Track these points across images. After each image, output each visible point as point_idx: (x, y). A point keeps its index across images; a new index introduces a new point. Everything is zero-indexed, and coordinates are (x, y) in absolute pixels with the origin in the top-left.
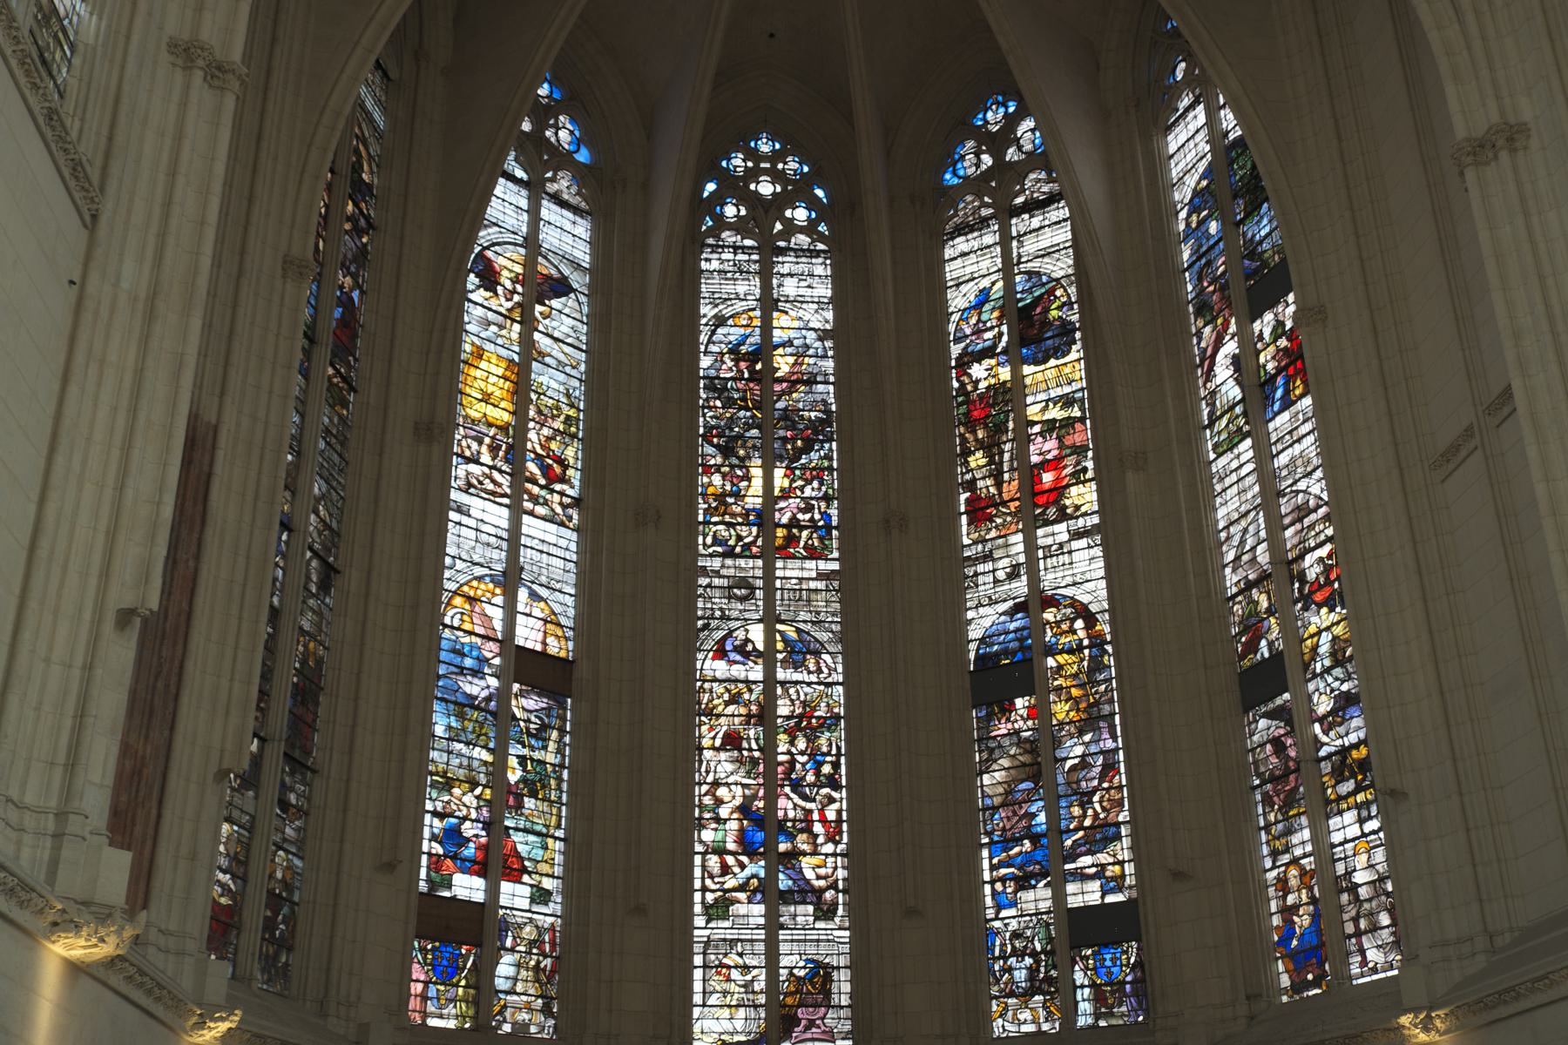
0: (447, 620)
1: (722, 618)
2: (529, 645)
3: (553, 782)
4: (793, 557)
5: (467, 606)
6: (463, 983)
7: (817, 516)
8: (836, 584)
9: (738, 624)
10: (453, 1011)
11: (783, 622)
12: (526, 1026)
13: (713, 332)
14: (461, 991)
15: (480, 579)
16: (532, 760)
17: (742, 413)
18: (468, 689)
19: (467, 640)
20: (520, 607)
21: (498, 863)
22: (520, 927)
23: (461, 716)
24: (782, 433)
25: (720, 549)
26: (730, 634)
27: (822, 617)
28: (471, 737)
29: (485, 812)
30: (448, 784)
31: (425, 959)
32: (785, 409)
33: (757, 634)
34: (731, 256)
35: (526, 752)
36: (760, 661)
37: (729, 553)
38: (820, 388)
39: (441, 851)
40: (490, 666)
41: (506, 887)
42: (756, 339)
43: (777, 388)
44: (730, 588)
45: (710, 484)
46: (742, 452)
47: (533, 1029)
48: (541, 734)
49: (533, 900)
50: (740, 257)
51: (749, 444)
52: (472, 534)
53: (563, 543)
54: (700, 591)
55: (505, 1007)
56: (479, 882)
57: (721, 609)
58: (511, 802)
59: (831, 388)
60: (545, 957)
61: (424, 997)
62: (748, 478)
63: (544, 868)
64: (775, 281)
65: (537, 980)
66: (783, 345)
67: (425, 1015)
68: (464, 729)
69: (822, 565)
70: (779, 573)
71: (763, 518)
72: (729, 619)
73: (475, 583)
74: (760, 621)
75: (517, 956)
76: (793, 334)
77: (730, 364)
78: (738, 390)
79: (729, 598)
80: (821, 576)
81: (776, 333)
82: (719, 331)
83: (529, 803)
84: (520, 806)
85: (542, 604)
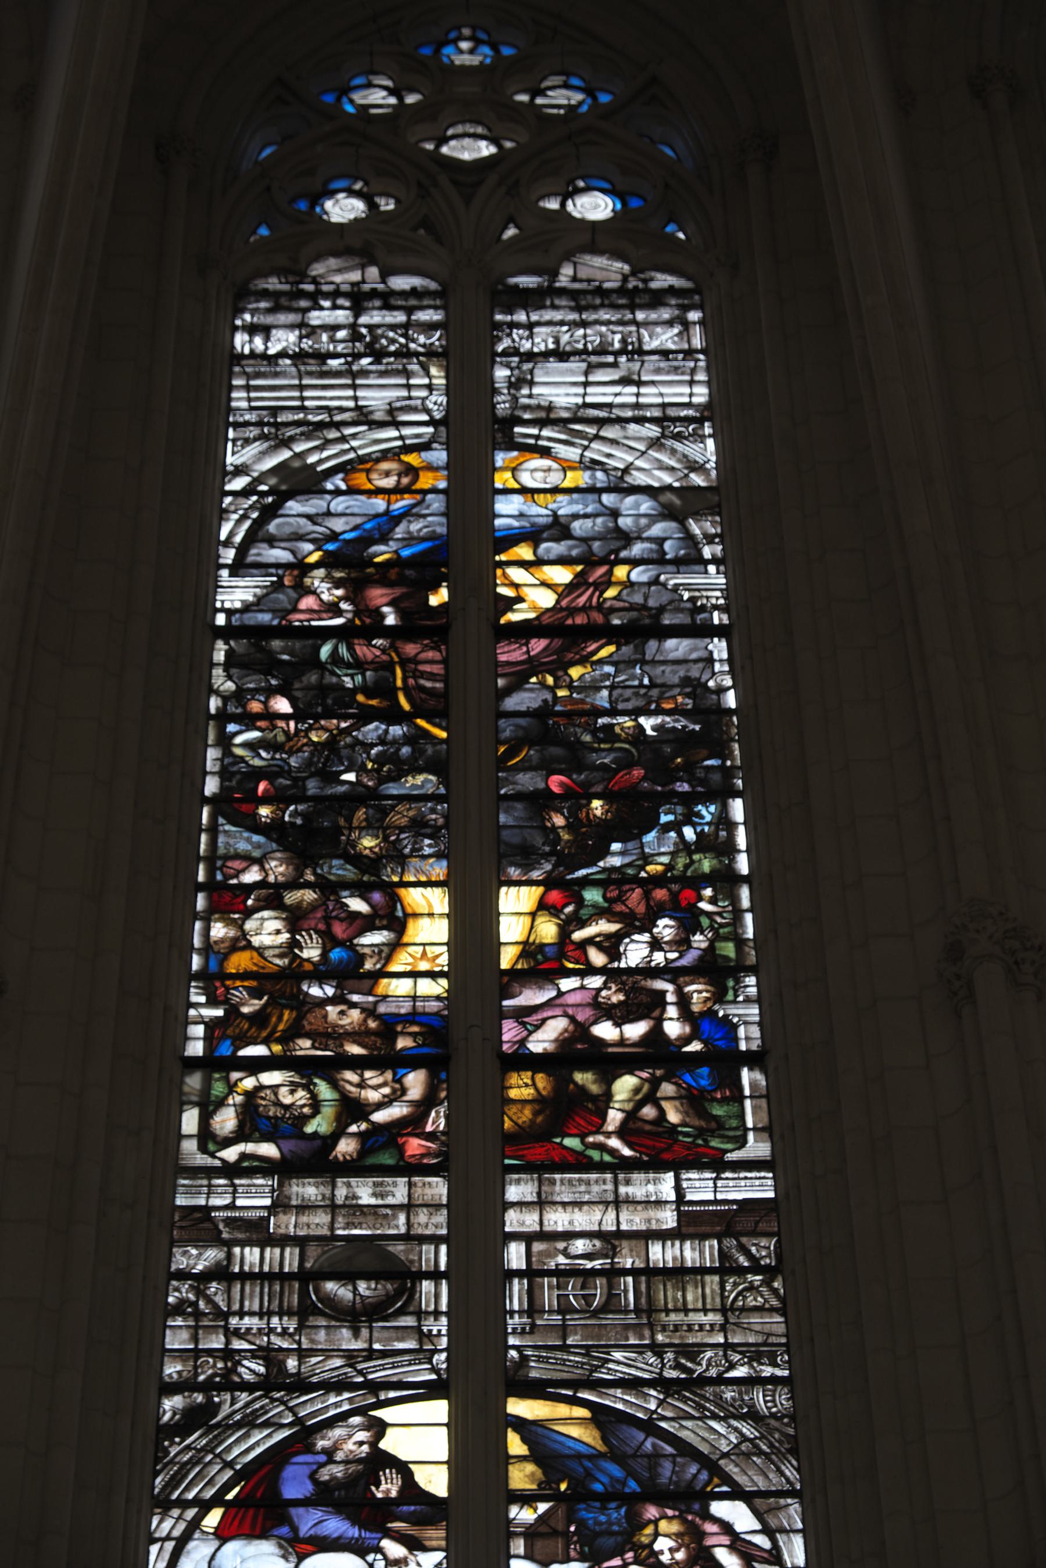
1: (265, 1385)
4: (580, 1163)
7: (673, 1029)
8: (764, 1248)
9: (338, 1402)
11: (536, 1390)
13: (269, 512)
17: (372, 730)
24: (528, 781)
25: (269, 1150)
26: (304, 1435)
27: (707, 1364)
32: (543, 713)
33: (421, 1438)
34: (342, 316)
36: (436, 1535)
37: (314, 1160)
38: (676, 647)
42: (431, 520)
43: (510, 653)
44: (305, 1277)
45: (241, 943)
46: (368, 842)
50: (374, 317)
51: (401, 816)
54: (179, 1293)
57: (268, 1355)
59: (719, 648)
62: (395, 920)
64: (501, 373)
66: (533, 535)
69: (701, 1188)
70: (514, 1221)
71: (455, 1042)
72: (301, 1385)
74: (430, 1391)
76: (565, 506)
77: (328, 593)
78: (359, 665)
79: (305, 1312)
80: (693, 1223)
81: (507, 507)
82: (293, 506)
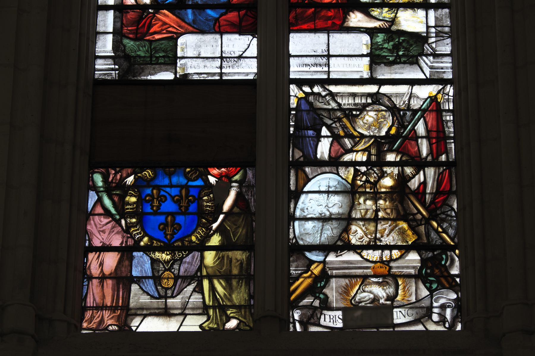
6: (215, 240)
14: (210, 257)
22: (351, 115)
41: (300, 43)
49: (376, 58)
55: (325, 276)
60: (420, 165)
61: (123, 279)
65: (402, 214)
67: (126, 312)
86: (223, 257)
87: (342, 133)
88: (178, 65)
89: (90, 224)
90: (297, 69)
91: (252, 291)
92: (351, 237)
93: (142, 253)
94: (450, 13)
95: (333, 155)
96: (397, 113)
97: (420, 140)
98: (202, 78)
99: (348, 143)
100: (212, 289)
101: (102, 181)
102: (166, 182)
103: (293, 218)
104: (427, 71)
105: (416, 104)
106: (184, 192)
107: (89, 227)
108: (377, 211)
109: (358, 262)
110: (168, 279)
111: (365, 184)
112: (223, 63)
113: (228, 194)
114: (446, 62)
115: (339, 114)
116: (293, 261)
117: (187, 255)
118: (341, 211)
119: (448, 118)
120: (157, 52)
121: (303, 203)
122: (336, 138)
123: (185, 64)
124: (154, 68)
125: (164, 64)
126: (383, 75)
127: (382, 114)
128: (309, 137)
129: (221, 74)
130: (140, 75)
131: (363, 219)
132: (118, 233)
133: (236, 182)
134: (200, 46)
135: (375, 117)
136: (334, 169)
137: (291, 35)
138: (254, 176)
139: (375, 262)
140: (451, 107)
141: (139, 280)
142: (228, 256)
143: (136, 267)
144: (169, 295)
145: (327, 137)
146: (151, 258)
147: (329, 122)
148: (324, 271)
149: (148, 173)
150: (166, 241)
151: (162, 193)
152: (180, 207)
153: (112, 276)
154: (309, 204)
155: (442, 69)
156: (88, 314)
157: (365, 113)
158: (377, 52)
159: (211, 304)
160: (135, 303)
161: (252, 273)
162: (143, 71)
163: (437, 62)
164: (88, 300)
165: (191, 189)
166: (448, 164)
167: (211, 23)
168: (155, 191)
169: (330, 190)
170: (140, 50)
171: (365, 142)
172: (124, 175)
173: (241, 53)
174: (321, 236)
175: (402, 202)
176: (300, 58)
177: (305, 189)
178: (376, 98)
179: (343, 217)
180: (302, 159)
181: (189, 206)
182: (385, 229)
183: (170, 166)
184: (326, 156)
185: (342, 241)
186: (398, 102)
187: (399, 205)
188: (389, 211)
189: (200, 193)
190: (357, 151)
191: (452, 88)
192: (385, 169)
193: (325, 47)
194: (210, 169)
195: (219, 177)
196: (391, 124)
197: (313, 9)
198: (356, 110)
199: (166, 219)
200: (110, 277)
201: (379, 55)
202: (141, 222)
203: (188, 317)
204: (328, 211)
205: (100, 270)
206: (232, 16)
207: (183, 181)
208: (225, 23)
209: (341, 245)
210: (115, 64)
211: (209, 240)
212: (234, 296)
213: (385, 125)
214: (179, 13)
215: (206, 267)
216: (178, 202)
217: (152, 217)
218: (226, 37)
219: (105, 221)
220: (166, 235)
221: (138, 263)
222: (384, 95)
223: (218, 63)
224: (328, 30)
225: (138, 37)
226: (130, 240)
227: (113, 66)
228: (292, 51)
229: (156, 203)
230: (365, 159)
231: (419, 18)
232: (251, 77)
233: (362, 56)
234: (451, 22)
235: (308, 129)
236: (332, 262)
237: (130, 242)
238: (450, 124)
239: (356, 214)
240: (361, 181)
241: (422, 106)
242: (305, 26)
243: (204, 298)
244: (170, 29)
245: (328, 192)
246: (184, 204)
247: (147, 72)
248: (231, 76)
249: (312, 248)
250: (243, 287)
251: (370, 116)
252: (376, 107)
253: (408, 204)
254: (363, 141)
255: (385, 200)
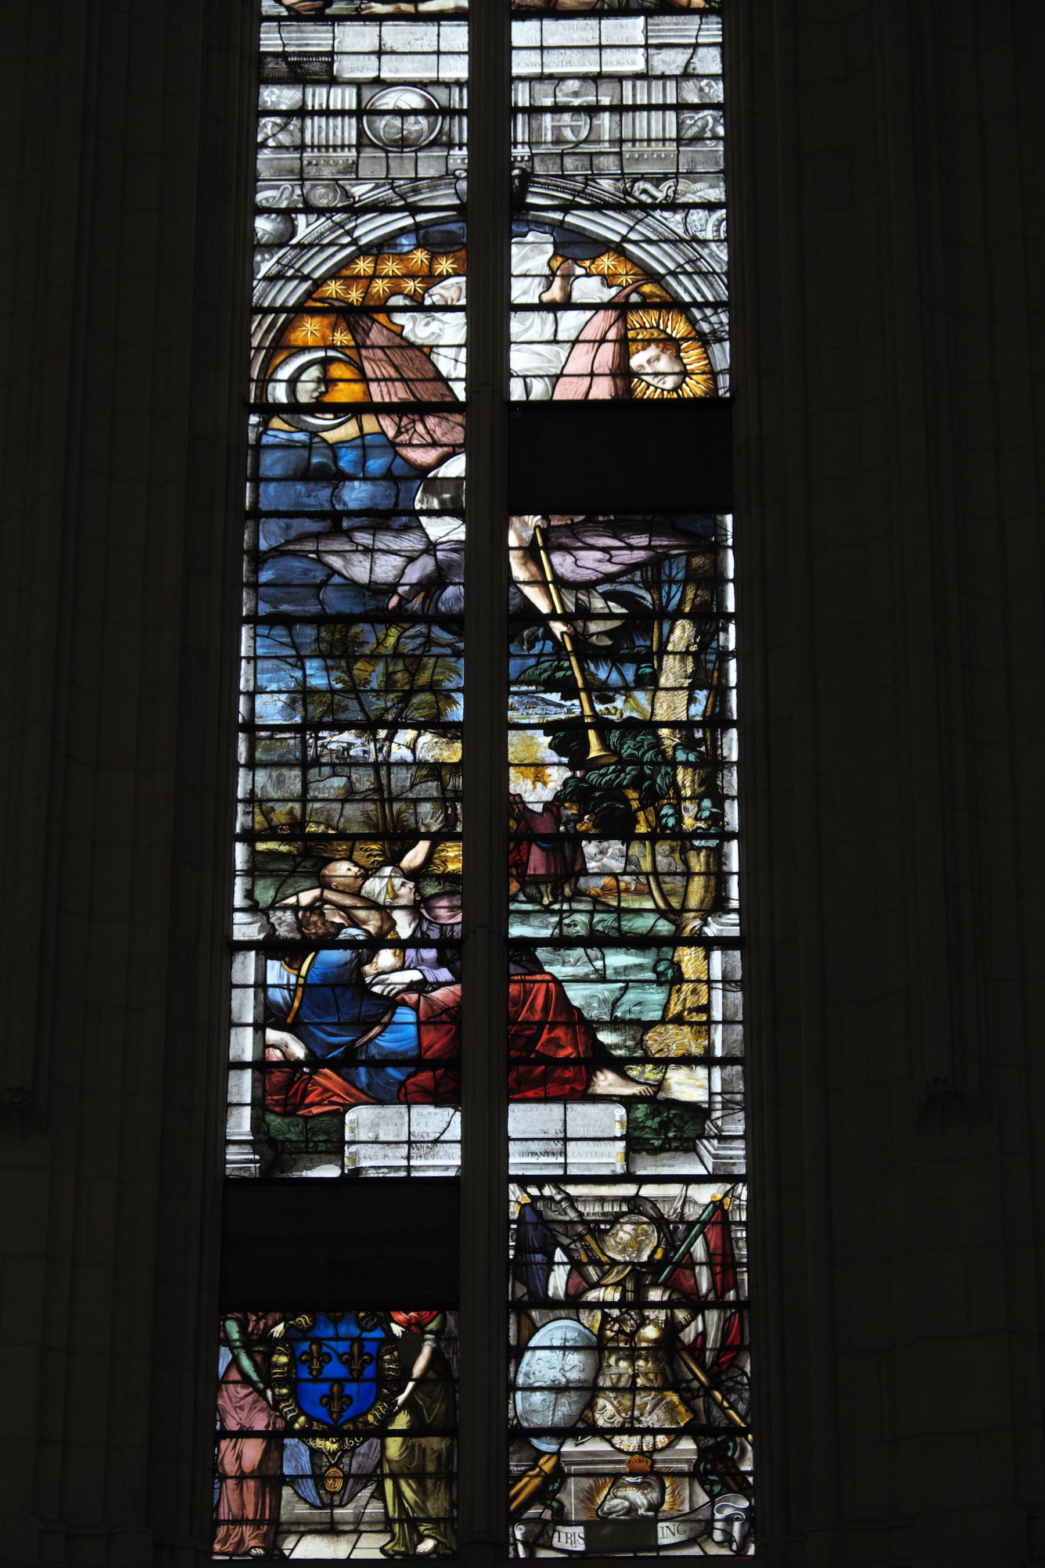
0: (279, 393)
2: (569, 391)
3: (684, 777)
5: (342, 338)
6: (402, 1421)
10: (375, 1509)
12: (640, 1526)
14: (394, 1447)
15: (380, 248)
16: (603, 726)
18: (360, 570)
19: (349, 430)
20: (522, 291)
21: (504, 1046)
22: (599, 1229)
23: (340, 653)
28: (376, 704)
29: (447, 914)
30: (307, 853)
31: (264, 1368)
35: (578, 707)
39: (298, 1050)
40: (433, 486)
41: (525, 1119)
47: (667, 1534)
48: (634, 644)
49: (635, 1143)
52: (347, 130)
53: (671, 62)
55: (559, 1475)
56: (439, 1121)
58: (537, 862)
60: (697, 1306)
63: (679, 1040)
65: (670, 1380)
68: (354, 689)
73: (364, 266)
75: (593, 1319)
83: (602, 856)
84: (568, 870)
85: (606, 263)
86: (413, 1446)
87: (584, 1259)
88: (347, 1154)
89: (223, 1397)
90: (519, 1160)
91: (455, 1497)
92: (597, 1416)
93: (296, 1440)
94: (743, 1072)
95: (572, 1291)
96: (664, 1227)
97: (697, 1268)
98: (381, 1175)
99: (592, 1272)
100: (398, 1493)
101: (239, 1332)
102: (330, 1332)
103: (513, 1388)
104: (709, 1162)
105: (692, 1213)
106: (356, 1347)
107: (220, 1402)
108: (634, 1376)
109: (606, 1453)
110: (334, 1478)
111: (617, 1335)
112: (412, 1151)
113: (419, 1352)
114: (737, 1149)
115: (580, 1229)
116: (514, 1453)
117: (362, 1443)
118: (582, 1376)
119: (739, 1235)
120: (315, 1134)
121: (527, 1364)
122: (576, 1266)
123: (356, 1153)
124: (311, 1159)
125: (327, 1152)
126: (645, 1168)
127: (643, 1229)
128: (536, 1264)
129: (409, 1168)
130: (291, 1169)
131: (614, 1389)
132: (262, 1410)
133: (431, 1332)
134: (378, 1125)
135: (632, 1232)
136: (572, 1313)
137: (512, 1107)
138: (458, 1323)
139: (631, 1454)
140: (744, 1218)
141: (293, 1481)
142: (420, 1445)
143: (289, 1461)
144: (337, 1503)
145: (563, 1263)
146: (310, 1448)
147: (566, 1241)
148: (557, 1467)
149: (304, 1320)
150: (332, 1422)
151: (325, 1349)
152: (351, 1371)
153: (255, 1474)
154: (537, 1367)
155: (731, 1158)
156: (222, 1531)
157: (618, 1226)
158: (637, 1134)
159: (396, 1516)
160: (287, 1516)
161: (455, 1470)
162: (295, 1164)
163: (724, 1149)
164: (221, 1510)
165: (366, 1343)
166: (738, 1305)
167: (394, 1089)
168: (314, 1347)
169: (567, 1344)
170: (290, 1131)
171: (618, 1272)
172: (270, 1323)
173: (437, 1135)
174: (553, 1414)
175: (671, 1362)
176: (524, 1143)
177: (532, 1344)
178: (635, 1204)
179: (586, 1385)
180: (526, 1298)
181: (364, 1368)
182: (646, 1404)
183: (335, 1309)
184: (561, 1293)
185: (584, 1421)
186: (667, 1210)
187: (667, 1368)
188: (651, 1376)
189: (379, 1350)
190: (607, 1286)
191: (745, 1188)
192: (646, 1313)
193: (560, 1126)
194: (393, 1314)
195: (407, 1325)
196: (655, 1244)
197: (543, 1067)
198: (605, 1222)
199: (331, 1387)
200: (251, 1476)
201: (639, 1138)
202: (294, 1394)
203: (364, 1535)
204: (564, 1376)
205: (237, 1466)
206: (425, 1077)
207: (355, 1331)
208: (414, 1088)
209: (583, 1427)
210: (254, 1153)
211: (392, 1421)
212: (429, 1504)
213: (648, 1245)
214: (347, 1073)
215: (389, 1461)
216: (348, 1363)
217: (311, 1386)
218: (416, 1110)
219: (243, 1392)
220: (331, 1413)
221: (292, 1455)
222: (646, 1198)
223: (404, 1150)
224: (565, 1099)
225: (288, 1111)
226: (279, 1420)
227: (251, 1157)
228: (512, 1134)
229: (316, 1365)
230: (617, 1297)
231: (697, 1080)
232: (452, 1173)
233: (615, 1139)
234: (745, 1086)
235: (535, 1252)
236: (569, 1454)
237: (280, 1424)
238: (742, 1244)
239: (605, 1381)
240: (612, 1331)
241: (701, 1216)
242: (530, 1094)
243: (386, 1507)
244: (334, 1099)
245: (564, 1348)
246: (356, 1366)
247: (301, 1164)
248: (424, 1171)
249: (541, 1432)
250: (442, 1490)
251: (626, 1232)
252: (634, 1218)
253: (680, 1366)
254: (616, 1270)
255: (646, 1360)
